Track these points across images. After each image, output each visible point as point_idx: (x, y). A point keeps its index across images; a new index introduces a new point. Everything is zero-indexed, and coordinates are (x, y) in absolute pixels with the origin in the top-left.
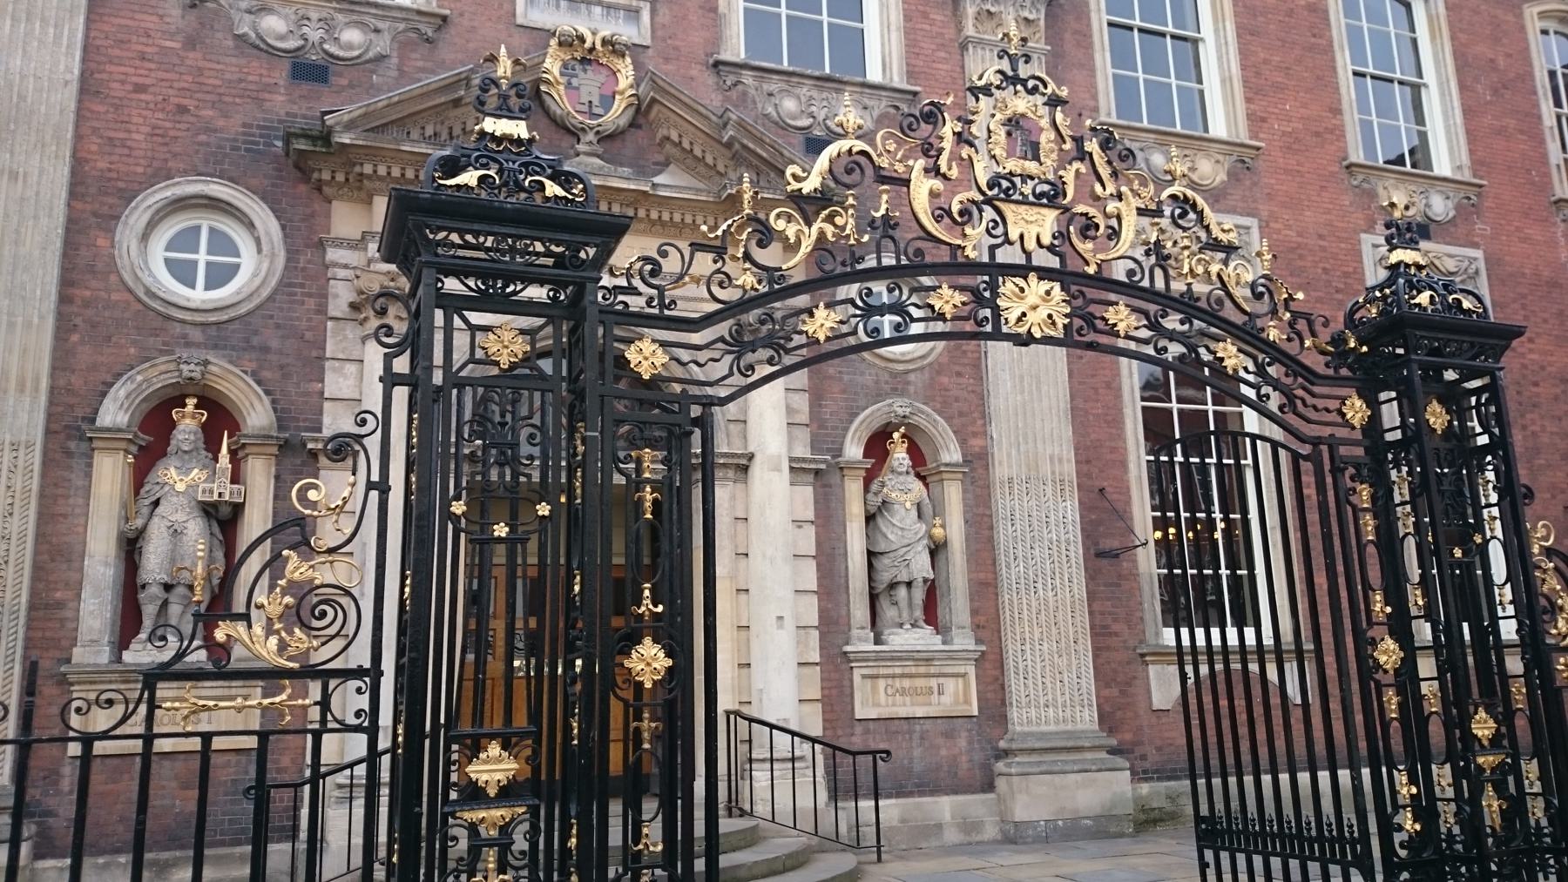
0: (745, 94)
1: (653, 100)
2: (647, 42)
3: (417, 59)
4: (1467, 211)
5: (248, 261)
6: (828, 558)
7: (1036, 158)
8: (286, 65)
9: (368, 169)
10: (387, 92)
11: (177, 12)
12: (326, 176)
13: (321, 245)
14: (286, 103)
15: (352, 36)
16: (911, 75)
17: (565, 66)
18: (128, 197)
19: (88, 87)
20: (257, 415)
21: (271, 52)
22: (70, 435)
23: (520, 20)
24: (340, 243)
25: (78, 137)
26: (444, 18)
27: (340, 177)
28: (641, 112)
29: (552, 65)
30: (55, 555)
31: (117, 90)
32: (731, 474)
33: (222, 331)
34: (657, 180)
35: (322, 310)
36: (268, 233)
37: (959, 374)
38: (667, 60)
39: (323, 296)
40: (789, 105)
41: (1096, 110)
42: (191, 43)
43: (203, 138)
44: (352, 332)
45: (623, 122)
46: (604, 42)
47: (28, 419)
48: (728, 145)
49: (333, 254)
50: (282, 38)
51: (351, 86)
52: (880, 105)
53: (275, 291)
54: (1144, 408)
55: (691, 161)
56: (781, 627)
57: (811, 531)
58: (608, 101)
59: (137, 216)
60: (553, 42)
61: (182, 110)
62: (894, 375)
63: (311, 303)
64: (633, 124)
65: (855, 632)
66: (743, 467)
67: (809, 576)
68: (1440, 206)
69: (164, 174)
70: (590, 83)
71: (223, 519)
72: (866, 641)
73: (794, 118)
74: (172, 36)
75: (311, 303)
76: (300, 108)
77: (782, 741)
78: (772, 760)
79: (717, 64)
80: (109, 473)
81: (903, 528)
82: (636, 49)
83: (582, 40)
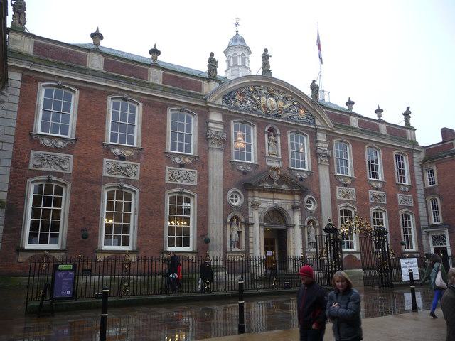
4: (384, 185)
5: (238, 201)
6: (303, 239)
14: (242, 178)
15: (249, 168)
19: (224, 178)
20: (243, 220)
22: (225, 223)
30: (225, 237)
33: (239, 209)
47: (221, 221)
55: (287, 184)
66: (294, 227)
68: (380, 186)
71: (239, 233)
80: (228, 226)
81: (312, 235)
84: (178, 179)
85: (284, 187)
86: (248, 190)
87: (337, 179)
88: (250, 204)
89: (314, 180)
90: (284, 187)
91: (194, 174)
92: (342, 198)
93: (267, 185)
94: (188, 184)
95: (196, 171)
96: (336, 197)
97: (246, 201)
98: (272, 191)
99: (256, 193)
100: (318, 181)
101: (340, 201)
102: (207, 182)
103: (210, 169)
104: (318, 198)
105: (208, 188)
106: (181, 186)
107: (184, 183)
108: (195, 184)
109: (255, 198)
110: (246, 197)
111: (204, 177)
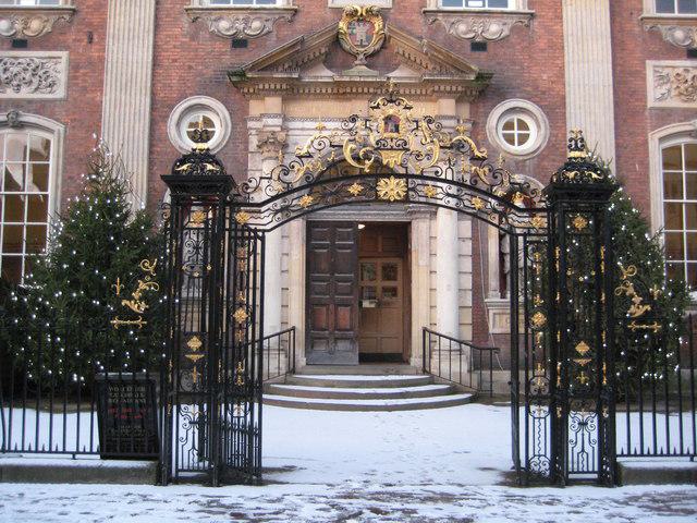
0: (440, 25)
1: (390, 37)
2: (390, 6)
3: (285, 32)
7: (397, 130)
8: (230, 42)
9: (261, 87)
10: (272, 47)
11: (187, 25)
12: (246, 91)
13: (245, 121)
14: (230, 59)
15: (256, 24)
16: (531, 4)
17: (350, 24)
18: (171, 107)
19: (155, 63)
21: (222, 37)
23: (330, 5)
24: (252, 119)
25: (153, 85)
26: (296, 11)
27: (251, 91)
28: (386, 40)
29: (342, 25)
31: (166, 63)
32: (428, 216)
34: (390, 75)
35: (246, 149)
36: (225, 117)
37: (554, 160)
38: (401, 13)
39: (247, 142)
40: (462, 28)
41: (641, 10)
42: (194, 37)
43: (198, 79)
44: (258, 158)
45: (377, 47)
46: (367, 11)
48: (426, 54)
49: (250, 124)
50: (228, 30)
51: (257, 47)
52: (511, 21)
53: (228, 142)
54: (664, 174)
56: (449, 290)
57: (470, 243)
58: (369, 39)
59: (175, 116)
60: (344, 14)
61: (190, 67)
62: (517, 163)
63: (242, 146)
64: (383, 47)
65: (491, 293)
67: (468, 265)
69: (183, 97)
70: (360, 31)
72: (496, 296)
73: (466, 33)
74: (185, 36)
75: (242, 146)
76: (234, 61)
77: (445, 342)
78: (450, 351)
79: (424, 12)
82: (382, 13)
83: (356, 11)
84: (8, 82)
85: (399, 75)
86: (246, 97)
87: (654, 34)
88: (254, 141)
89: (542, 44)
90: (399, 75)
91: (59, 64)
92: (674, 103)
93: (325, 74)
94: (37, 96)
95: (64, 54)
96: (644, 98)
97: (239, 134)
98: (341, 92)
99: (273, 103)
100: (557, 47)
101: (665, 116)
102: (99, 85)
103: (110, 41)
104: (555, 110)
105: (99, 105)
106: (18, 104)
107: (25, 93)
108: (60, 92)
109: (270, 121)
110: (239, 118)
111: (89, 74)
